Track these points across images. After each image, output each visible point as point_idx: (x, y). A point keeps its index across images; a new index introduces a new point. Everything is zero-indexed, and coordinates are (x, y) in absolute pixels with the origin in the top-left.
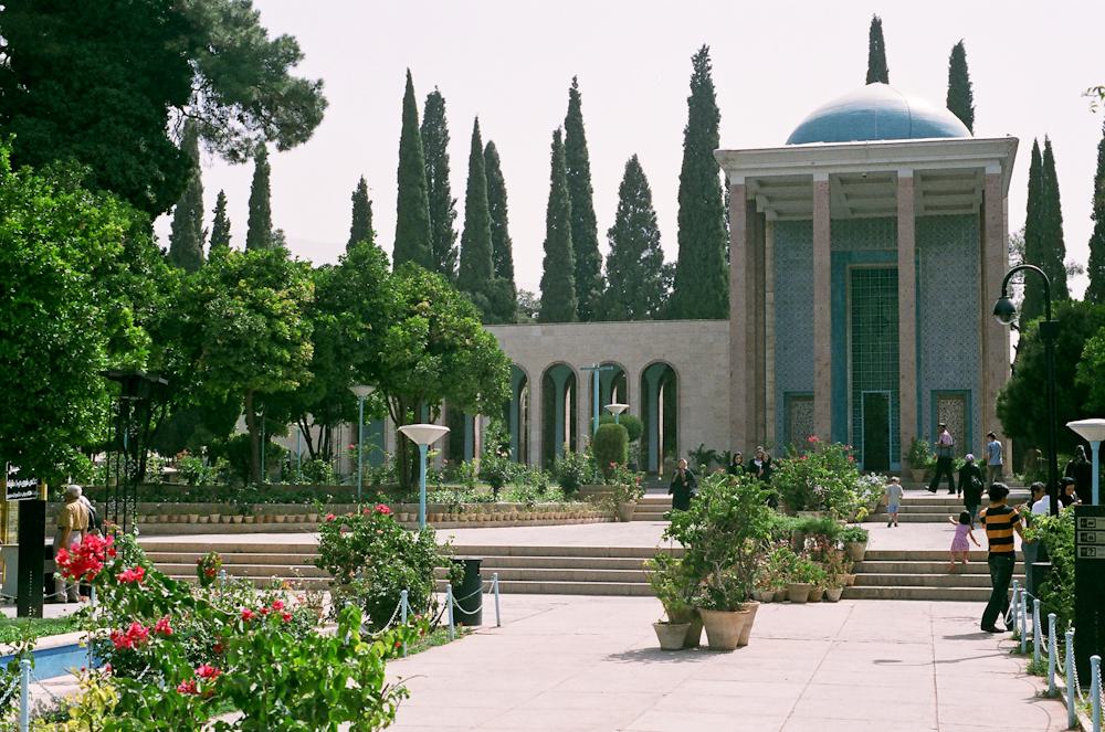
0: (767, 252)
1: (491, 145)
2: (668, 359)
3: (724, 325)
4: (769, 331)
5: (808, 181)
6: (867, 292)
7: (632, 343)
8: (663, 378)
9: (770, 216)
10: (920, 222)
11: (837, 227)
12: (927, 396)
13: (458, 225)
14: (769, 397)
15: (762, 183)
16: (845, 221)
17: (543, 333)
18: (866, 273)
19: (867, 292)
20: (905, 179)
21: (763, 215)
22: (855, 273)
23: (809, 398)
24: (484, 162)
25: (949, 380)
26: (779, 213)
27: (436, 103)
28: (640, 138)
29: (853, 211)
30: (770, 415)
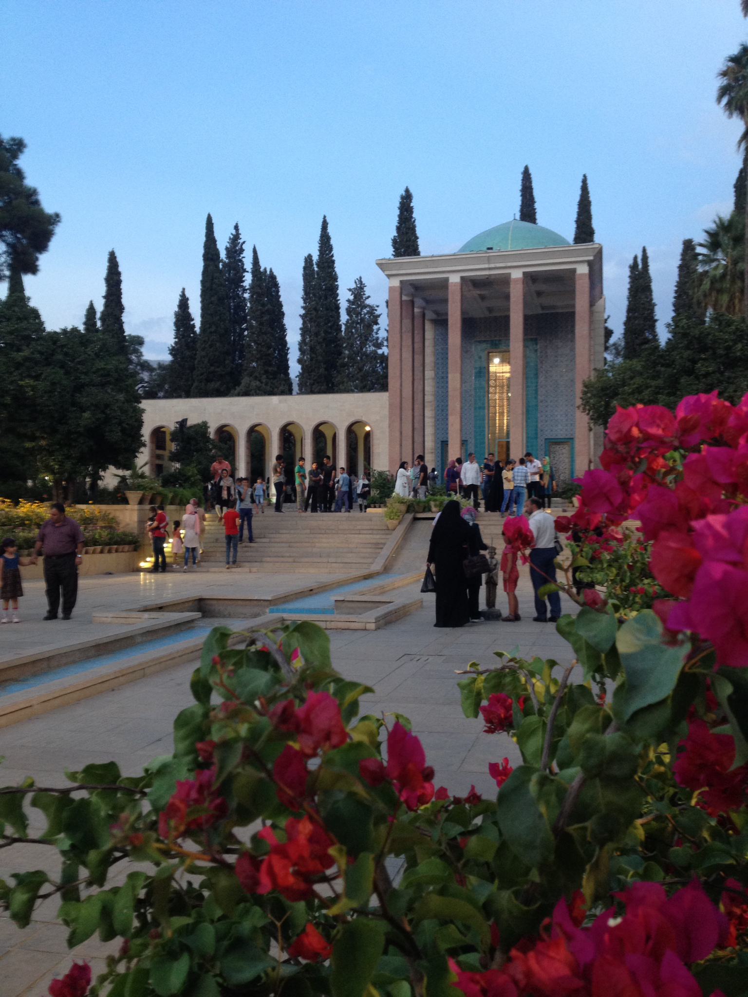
0: (427, 343)
1: (273, 277)
3: (383, 397)
4: (429, 398)
5: (444, 284)
12: (541, 442)
13: (293, 337)
17: (280, 402)
20: (516, 280)
24: (267, 285)
27: (235, 247)
29: (490, 310)
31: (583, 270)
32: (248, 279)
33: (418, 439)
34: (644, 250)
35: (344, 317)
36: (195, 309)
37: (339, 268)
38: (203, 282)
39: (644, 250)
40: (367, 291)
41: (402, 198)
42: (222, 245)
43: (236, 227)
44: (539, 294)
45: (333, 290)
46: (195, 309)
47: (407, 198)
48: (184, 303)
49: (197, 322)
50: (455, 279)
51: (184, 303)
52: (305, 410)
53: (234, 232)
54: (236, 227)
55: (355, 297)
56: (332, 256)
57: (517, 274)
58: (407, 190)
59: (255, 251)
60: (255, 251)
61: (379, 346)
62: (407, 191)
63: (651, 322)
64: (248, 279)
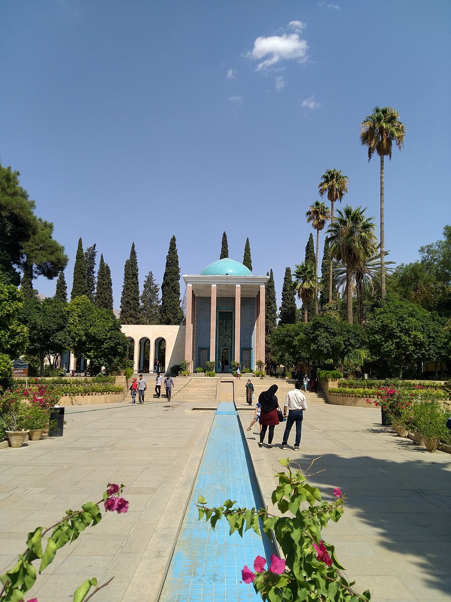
2: (163, 337)
7: (152, 332)
8: (161, 342)
11: (219, 299)
18: (223, 313)
20: (238, 287)
22: (220, 313)
24: (105, 271)
28: (152, 268)
31: (263, 287)
32: (97, 268)
34: (271, 270)
35: (141, 289)
37: (139, 266)
38: (75, 268)
39: (271, 270)
40: (154, 277)
41: (172, 239)
42: (85, 251)
43: (95, 246)
45: (135, 276)
47: (174, 239)
53: (93, 246)
54: (95, 246)
55: (148, 280)
56: (136, 260)
58: (174, 236)
59: (102, 256)
60: (102, 256)
61: (158, 302)
62: (174, 236)
63: (273, 299)
64: (97, 268)
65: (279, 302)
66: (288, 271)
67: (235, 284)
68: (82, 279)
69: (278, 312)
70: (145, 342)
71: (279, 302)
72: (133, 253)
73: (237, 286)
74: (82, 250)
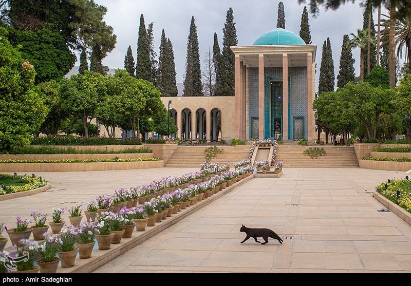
2: (218, 107)
4: (247, 99)
6: (275, 89)
8: (216, 113)
9: (247, 66)
10: (290, 69)
12: (292, 119)
14: (247, 118)
15: (244, 56)
16: (270, 68)
17: (182, 99)
19: (275, 89)
20: (285, 57)
21: (245, 66)
23: (258, 118)
24: (166, 46)
25: (298, 114)
26: (250, 65)
30: (247, 124)
33: (244, 117)
34: (328, 39)
36: (135, 55)
37: (199, 40)
39: (328, 39)
42: (147, 28)
44: (291, 60)
46: (135, 55)
48: (130, 52)
49: (135, 61)
50: (261, 55)
51: (130, 52)
52: (194, 103)
57: (285, 55)
65: (337, 71)
66: (346, 38)
67: (281, 53)
68: (145, 54)
69: (336, 81)
70: (201, 113)
71: (337, 71)
72: (193, 28)
73: (284, 55)
74: (144, 26)
